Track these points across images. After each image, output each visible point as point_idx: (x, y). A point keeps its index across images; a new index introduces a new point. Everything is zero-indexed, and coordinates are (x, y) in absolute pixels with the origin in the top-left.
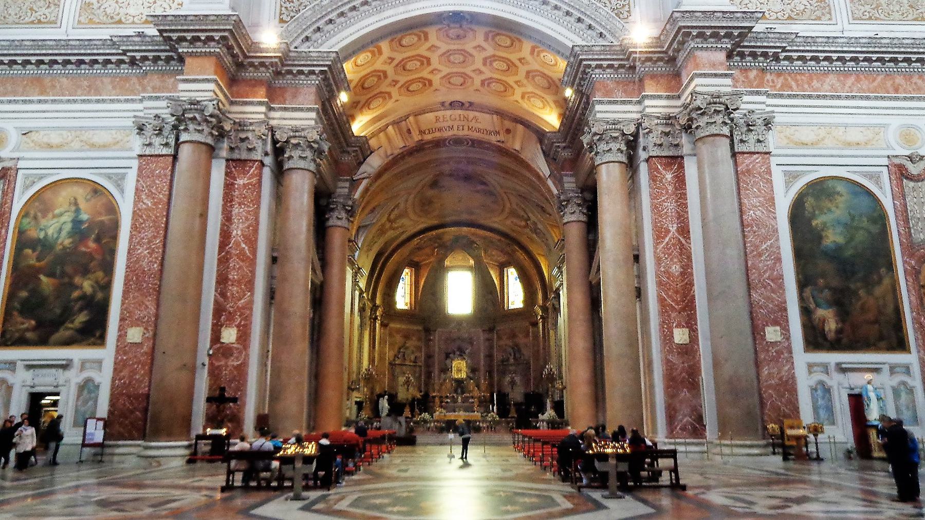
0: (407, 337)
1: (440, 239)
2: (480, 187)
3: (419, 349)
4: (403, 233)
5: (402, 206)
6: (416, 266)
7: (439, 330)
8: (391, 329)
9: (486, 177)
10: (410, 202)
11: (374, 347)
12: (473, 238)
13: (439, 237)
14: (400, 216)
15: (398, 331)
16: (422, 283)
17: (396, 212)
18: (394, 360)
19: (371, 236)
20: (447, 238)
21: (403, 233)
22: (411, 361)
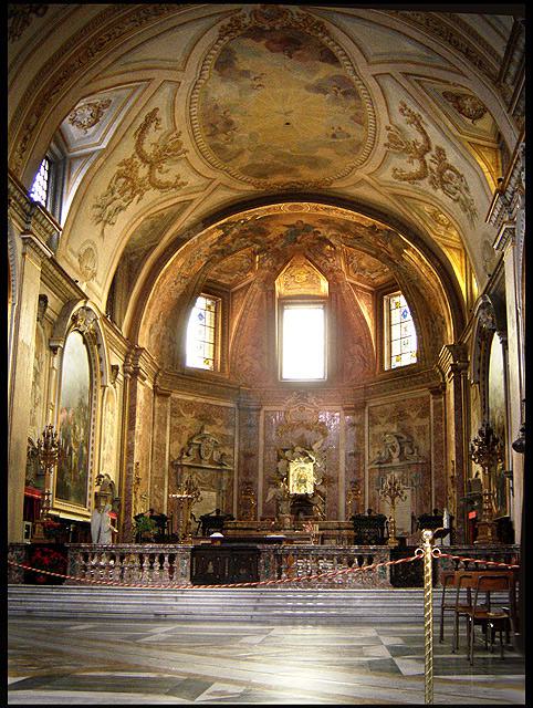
0: (205, 418)
1: (264, 233)
2: (325, 71)
3: (226, 441)
4: (184, 205)
5: (163, 116)
6: (222, 295)
7: (265, 408)
8: (175, 401)
9: (334, 30)
10: (181, 111)
11: (132, 426)
12: (324, 232)
13: (259, 229)
14: (169, 152)
15: (189, 407)
16: (235, 324)
17: (153, 136)
18: (180, 458)
19: (101, 186)
20: (276, 230)
21: (184, 205)
22: (211, 462)
